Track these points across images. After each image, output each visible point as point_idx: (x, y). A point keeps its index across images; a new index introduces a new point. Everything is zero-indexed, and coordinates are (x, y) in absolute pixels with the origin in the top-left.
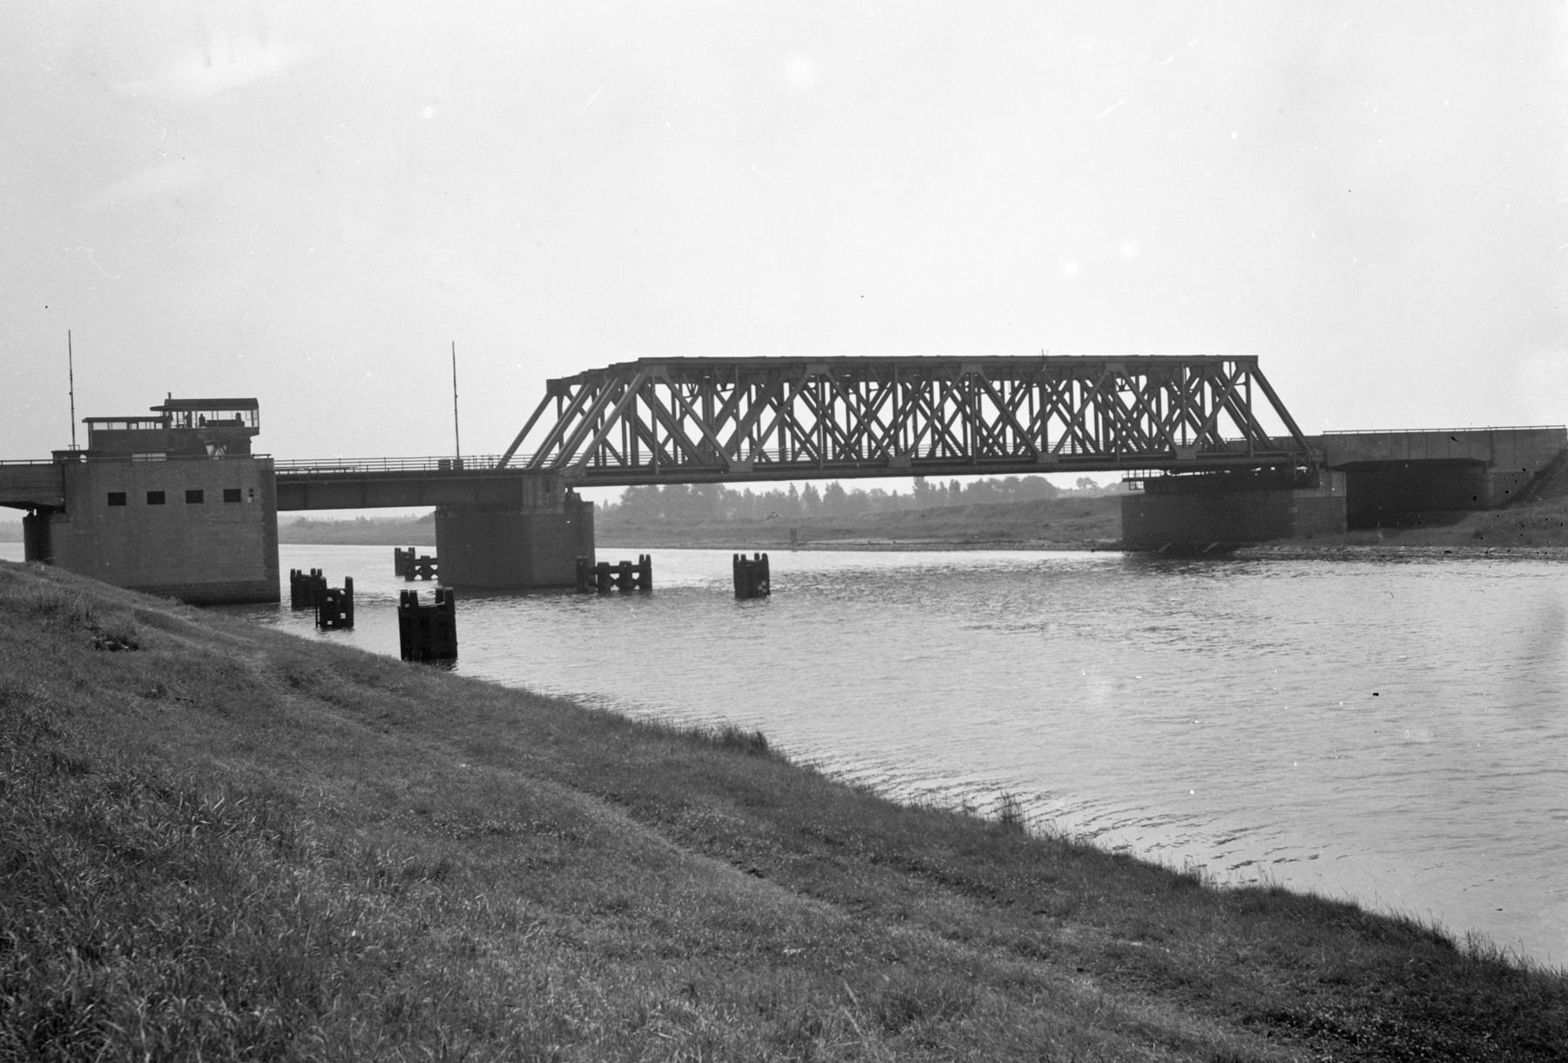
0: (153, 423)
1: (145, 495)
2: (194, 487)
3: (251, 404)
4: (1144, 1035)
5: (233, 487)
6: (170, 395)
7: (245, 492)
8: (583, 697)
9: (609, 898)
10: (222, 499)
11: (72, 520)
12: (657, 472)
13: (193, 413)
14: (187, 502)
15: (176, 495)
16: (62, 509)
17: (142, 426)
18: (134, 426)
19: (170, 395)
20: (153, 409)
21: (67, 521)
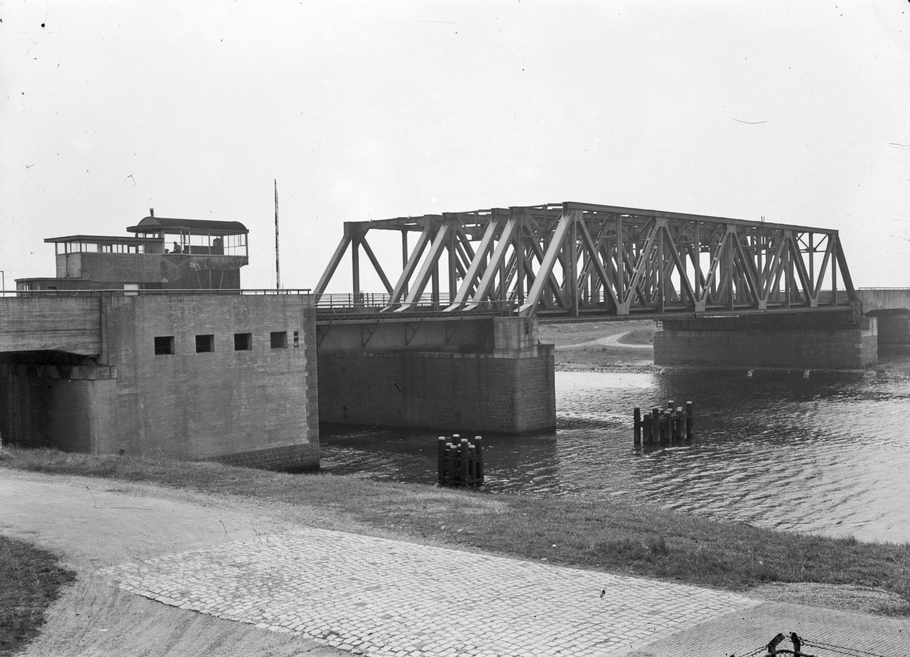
0: (126, 247)
1: (194, 340)
2: (243, 330)
3: (238, 228)
4: (724, 569)
5: (279, 329)
6: (152, 211)
7: (290, 337)
8: (78, 553)
9: (650, 552)
10: (268, 344)
11: (115, 375)
12: (577, 314)
13: (225, 238)
14: (236, 349)
15: (224, 339)
16: (95, 360)
17: (117, 249)
18: (106, 249)
19: (152, 211)
20: (130, 229)
21: (110, 377)
